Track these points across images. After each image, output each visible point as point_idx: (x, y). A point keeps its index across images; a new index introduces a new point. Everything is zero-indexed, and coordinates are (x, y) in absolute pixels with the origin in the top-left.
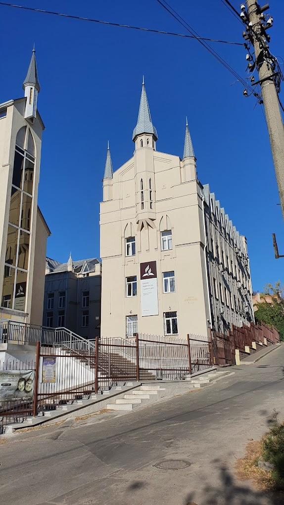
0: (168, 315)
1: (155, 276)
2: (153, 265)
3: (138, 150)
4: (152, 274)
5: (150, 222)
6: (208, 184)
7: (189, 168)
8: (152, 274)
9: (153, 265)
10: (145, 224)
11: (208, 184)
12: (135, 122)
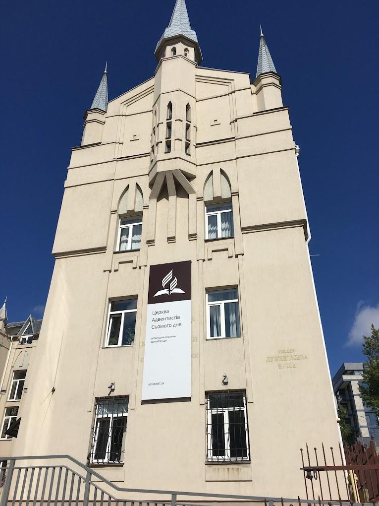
0: (215, 398)
1: (187, 296)
2: (182, 271)
3: (168, 59)
4: (180, 291)
5: (183, 180)
6: (52, 253)
7: (273, 96)
8: (180, 291)
9: (182, 271)
10: (171, 186)
11: (52, 253)
12: (166, 23)
